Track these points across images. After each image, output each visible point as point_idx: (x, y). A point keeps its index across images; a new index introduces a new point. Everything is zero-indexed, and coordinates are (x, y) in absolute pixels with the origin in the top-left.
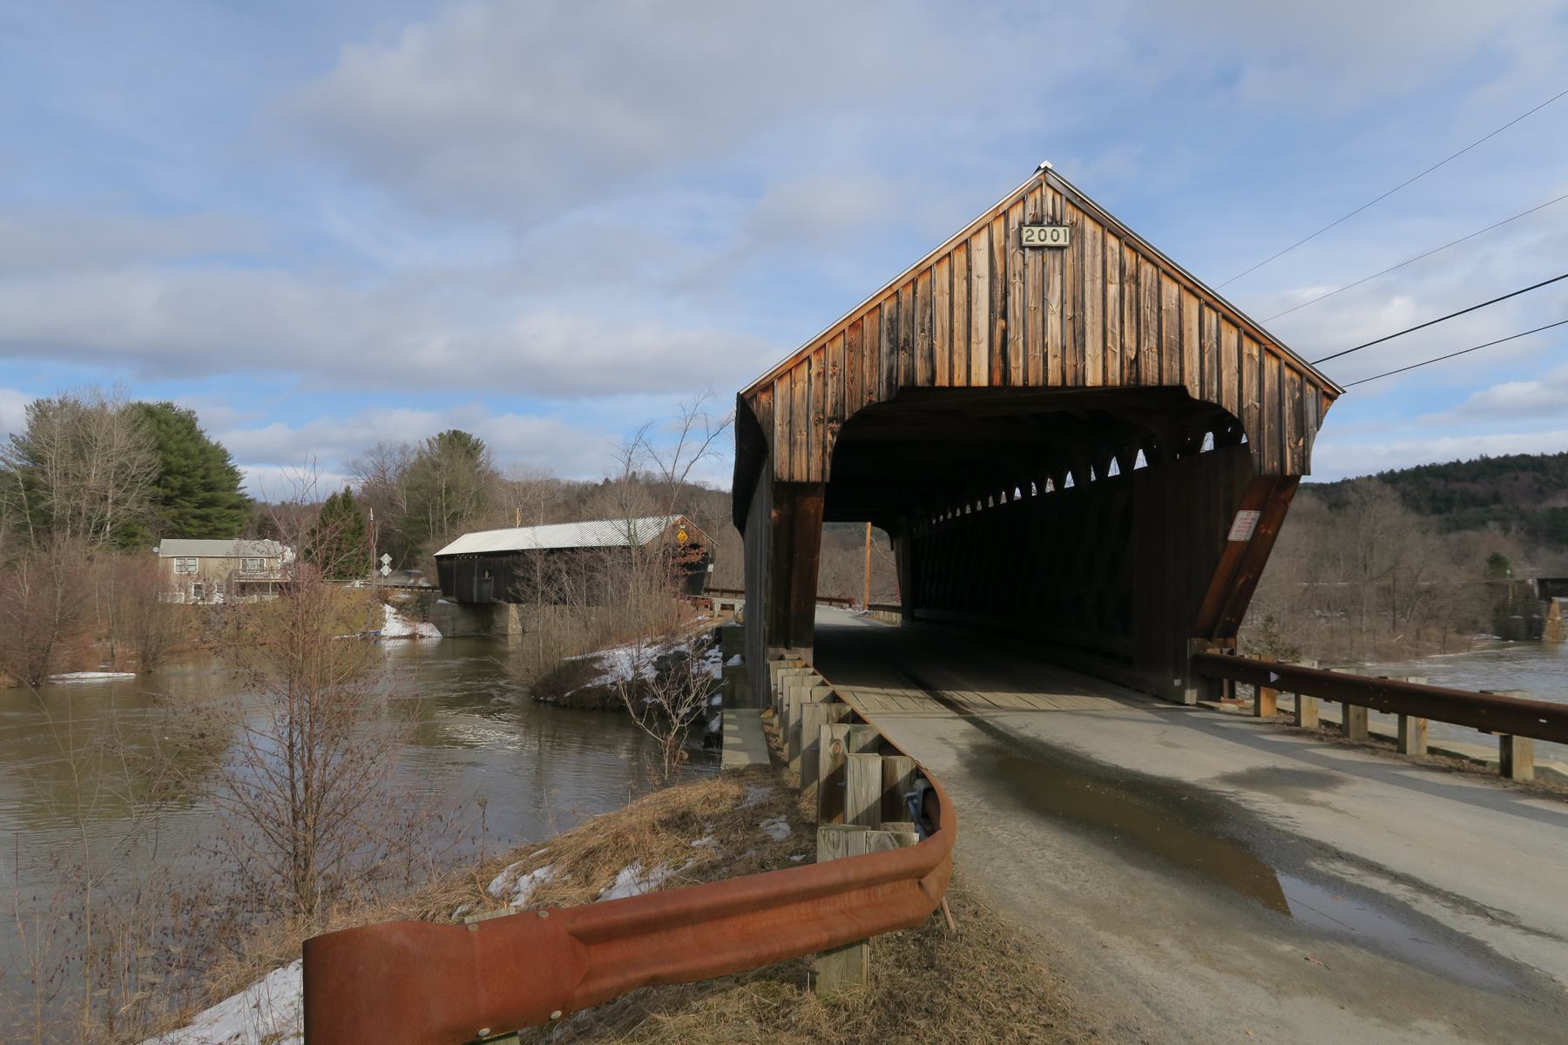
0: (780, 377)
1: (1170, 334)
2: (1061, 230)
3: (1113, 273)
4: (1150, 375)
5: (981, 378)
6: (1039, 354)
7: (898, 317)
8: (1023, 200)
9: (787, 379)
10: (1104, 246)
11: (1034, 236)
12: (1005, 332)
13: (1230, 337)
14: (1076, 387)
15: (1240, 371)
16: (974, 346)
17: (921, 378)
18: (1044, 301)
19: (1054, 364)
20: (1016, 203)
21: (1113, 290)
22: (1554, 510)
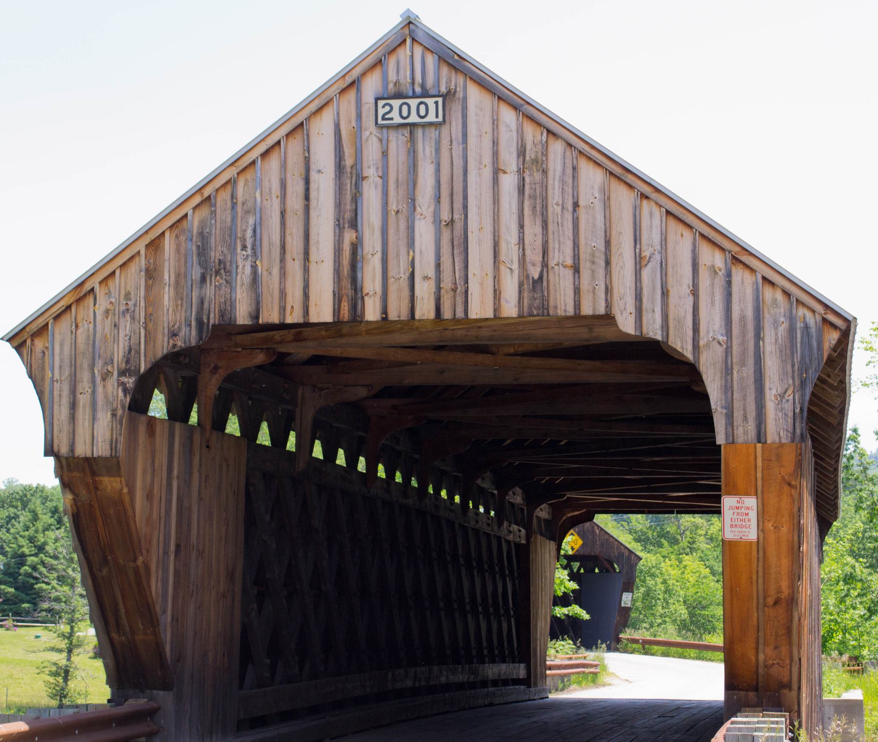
0: (57, 318)
1: (592, 241)
2: (430, 102)
3: (510, 160)
4: (562, 302)
5: (323, 312)
6: (404, 277)
7: (198, 230)
8: (379, 63)
9: (66, 320)
10: (495, 123)
11: (395, 112)
12: (355, 248)
13: (682, 243)
14: (455, 320)
15: (695, 292)
16: (313, 267)
17: (425, 310)
18: (412, 201)
19: (424, 291)
20: (373, 67)
21: (508, 182)
22: (28, 582)
